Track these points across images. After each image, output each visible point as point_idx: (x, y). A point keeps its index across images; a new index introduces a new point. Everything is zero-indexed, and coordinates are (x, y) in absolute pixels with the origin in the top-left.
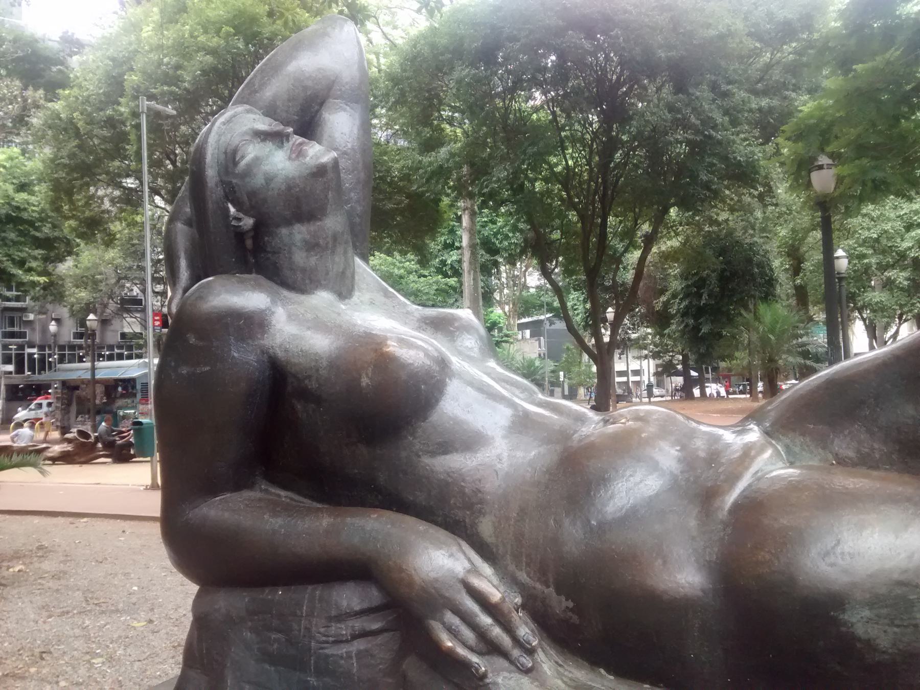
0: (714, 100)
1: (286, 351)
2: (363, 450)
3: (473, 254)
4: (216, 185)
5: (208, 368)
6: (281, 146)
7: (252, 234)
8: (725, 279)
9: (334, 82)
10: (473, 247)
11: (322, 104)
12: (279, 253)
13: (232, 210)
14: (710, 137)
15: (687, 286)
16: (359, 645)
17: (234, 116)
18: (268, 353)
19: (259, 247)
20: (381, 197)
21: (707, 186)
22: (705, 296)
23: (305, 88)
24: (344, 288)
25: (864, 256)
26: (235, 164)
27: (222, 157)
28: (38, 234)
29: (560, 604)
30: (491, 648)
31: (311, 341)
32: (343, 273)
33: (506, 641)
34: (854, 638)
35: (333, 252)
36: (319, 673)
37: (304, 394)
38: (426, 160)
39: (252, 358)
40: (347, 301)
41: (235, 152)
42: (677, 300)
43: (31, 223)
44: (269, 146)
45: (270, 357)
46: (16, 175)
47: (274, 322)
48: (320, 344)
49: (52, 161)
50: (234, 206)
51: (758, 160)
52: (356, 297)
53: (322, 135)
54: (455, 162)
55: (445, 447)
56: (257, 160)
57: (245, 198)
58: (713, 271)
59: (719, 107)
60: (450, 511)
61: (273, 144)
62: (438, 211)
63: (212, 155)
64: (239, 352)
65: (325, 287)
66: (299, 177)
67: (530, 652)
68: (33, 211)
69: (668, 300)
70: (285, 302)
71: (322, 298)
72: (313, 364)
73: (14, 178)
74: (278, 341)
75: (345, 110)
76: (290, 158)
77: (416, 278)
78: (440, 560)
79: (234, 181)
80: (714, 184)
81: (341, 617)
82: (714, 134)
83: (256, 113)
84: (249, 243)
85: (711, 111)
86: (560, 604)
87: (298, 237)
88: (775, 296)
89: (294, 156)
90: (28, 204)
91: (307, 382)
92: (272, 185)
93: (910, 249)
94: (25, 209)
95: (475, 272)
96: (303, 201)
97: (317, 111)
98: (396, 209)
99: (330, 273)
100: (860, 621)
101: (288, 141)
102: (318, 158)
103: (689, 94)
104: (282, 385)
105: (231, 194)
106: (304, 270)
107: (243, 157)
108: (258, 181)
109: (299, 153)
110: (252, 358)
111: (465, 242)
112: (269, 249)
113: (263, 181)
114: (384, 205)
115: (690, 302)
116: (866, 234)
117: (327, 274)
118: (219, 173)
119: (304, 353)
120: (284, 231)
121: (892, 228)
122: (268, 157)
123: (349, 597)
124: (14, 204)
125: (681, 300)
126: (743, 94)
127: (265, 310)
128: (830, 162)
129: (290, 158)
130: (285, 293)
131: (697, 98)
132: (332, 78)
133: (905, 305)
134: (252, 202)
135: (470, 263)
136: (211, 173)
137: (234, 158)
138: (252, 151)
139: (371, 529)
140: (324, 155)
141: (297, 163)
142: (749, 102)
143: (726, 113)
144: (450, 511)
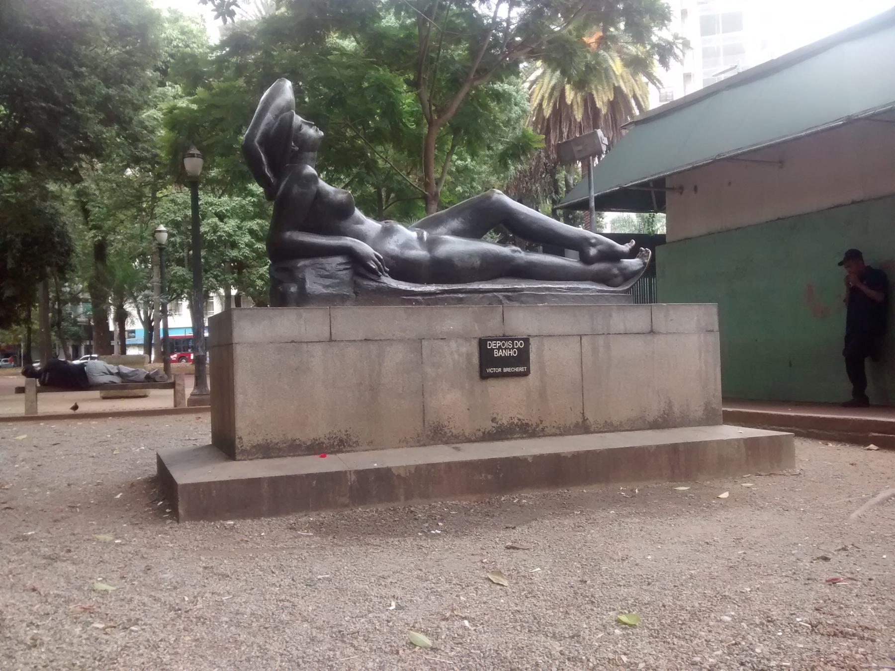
16: (344, 272)
36: (336, 278)
58: (17, 236)
88: (71, 265)
100: (456, 261)
123: (339, 259)
128: (198, 152)
139: (348, 241)
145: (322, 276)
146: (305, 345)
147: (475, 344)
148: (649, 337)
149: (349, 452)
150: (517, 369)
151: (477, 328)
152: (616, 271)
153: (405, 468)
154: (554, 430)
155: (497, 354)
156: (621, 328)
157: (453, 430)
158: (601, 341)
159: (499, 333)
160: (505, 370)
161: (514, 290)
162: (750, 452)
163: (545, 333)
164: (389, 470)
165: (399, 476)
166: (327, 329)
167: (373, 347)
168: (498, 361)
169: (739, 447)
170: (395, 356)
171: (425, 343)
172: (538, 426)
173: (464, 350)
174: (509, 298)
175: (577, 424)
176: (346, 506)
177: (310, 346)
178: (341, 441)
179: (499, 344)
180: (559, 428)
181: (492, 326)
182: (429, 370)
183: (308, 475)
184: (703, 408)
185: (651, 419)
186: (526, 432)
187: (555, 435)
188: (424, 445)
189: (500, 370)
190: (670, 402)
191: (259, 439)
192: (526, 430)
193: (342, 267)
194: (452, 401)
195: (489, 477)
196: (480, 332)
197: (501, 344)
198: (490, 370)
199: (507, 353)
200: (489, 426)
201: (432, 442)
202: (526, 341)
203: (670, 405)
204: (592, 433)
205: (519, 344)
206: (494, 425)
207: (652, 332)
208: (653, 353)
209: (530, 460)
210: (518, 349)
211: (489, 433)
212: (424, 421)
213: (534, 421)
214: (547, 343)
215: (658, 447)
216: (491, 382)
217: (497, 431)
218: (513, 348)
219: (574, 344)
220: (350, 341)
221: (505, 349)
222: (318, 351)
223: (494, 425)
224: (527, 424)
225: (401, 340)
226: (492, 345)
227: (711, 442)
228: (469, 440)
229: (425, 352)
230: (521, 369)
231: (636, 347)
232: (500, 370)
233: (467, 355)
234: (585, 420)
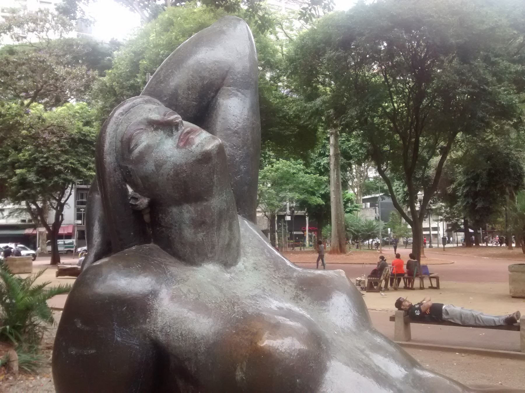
0: (486, 67)
1: (167, 334)
3: (336, 160)
4: (115, 171)
5: (93, 351)
6: (171, 135)
7: (148, 211)
9: (227, 72)
10: (336, 155)
11: (217, 91)
12: (171, 228)
13: (130, 190)
14: (484, 90)
15: (468, 179)
17: (133, 107)
18: (149, 337)
19: (155, 222)
20: (283, 128)
21: (482, 120)
22: (479, 185)
23: (202, 78)
24: (228, 257)
26: (130, 151)
27: (119, 144)
31: (190, 326)
32: (229, 245)
35: (219, 229)
37: (184, 374)
38: (309, 105)
39: (134, 342)
40: (232, 268)
41: (130, 140)
42: (462, 187)
43: (91, 143)
44: (160, 135)
45: (152, 340)
46: (84, 117)
47: (156, 306)
48: (201, 326)
49: (102, 109)
50: (132, 187)
51: (515, 103)
52: (240, 265)
53: (217, 118)
54: (326, 107)
56: (149, 148)
57: (140, 181)
59: (490, 72)
61: (164, 133)
63: (110, 143)
64: (122, 336)
65: (211, 260)
66: (186, 164)
68: (93, 136)
69: (456, 187)
72: (192, 348)
73: (83, 118)
74: (160, 324)
75: (236, 95)
76: (178, 147)
79: (130, 166)
80: (486, 118)
82: (487, 88)
83: (154, 103)
84: (147, 218)
85: (485, 74)
87: (186, 216)
89: (182, 144)
90: (90, 132)
91: (187, 363)
92: (162, 171)
94: (88, 135)
95: (337, 170)
96: (191, 184)
97: (213, 97)
98: (291, 135)
99: (216, 248)
101: (177, 129)
102: (203, 146)
103: (471, 64)
105: (128, 177)
106: (192, 245)
107: (136, 145)
108: (150, 167)
109: (186, 141)
110: (134, 342)
111: (332, 152)
112: (163, 224)
113: (153, 168)
114: (285, 133)
115: (470, 189)
117: (213, 247)
118: (116, 159)
120: (175, 210)
122: (158, 144)
124: (82, 132)
125: (464, 187)
126: (506, 63)
127: (148, 295)
129: (178, 147)
131: (476, 66)
132: (226, 69)
134: (146, 185)
135: (334, 165)
136: (109, 159)
137: (129, 147)
138: (145, 140)
140: (209, 143)
141: (184, 150)
142: (509, 67)
143: (494, 74)
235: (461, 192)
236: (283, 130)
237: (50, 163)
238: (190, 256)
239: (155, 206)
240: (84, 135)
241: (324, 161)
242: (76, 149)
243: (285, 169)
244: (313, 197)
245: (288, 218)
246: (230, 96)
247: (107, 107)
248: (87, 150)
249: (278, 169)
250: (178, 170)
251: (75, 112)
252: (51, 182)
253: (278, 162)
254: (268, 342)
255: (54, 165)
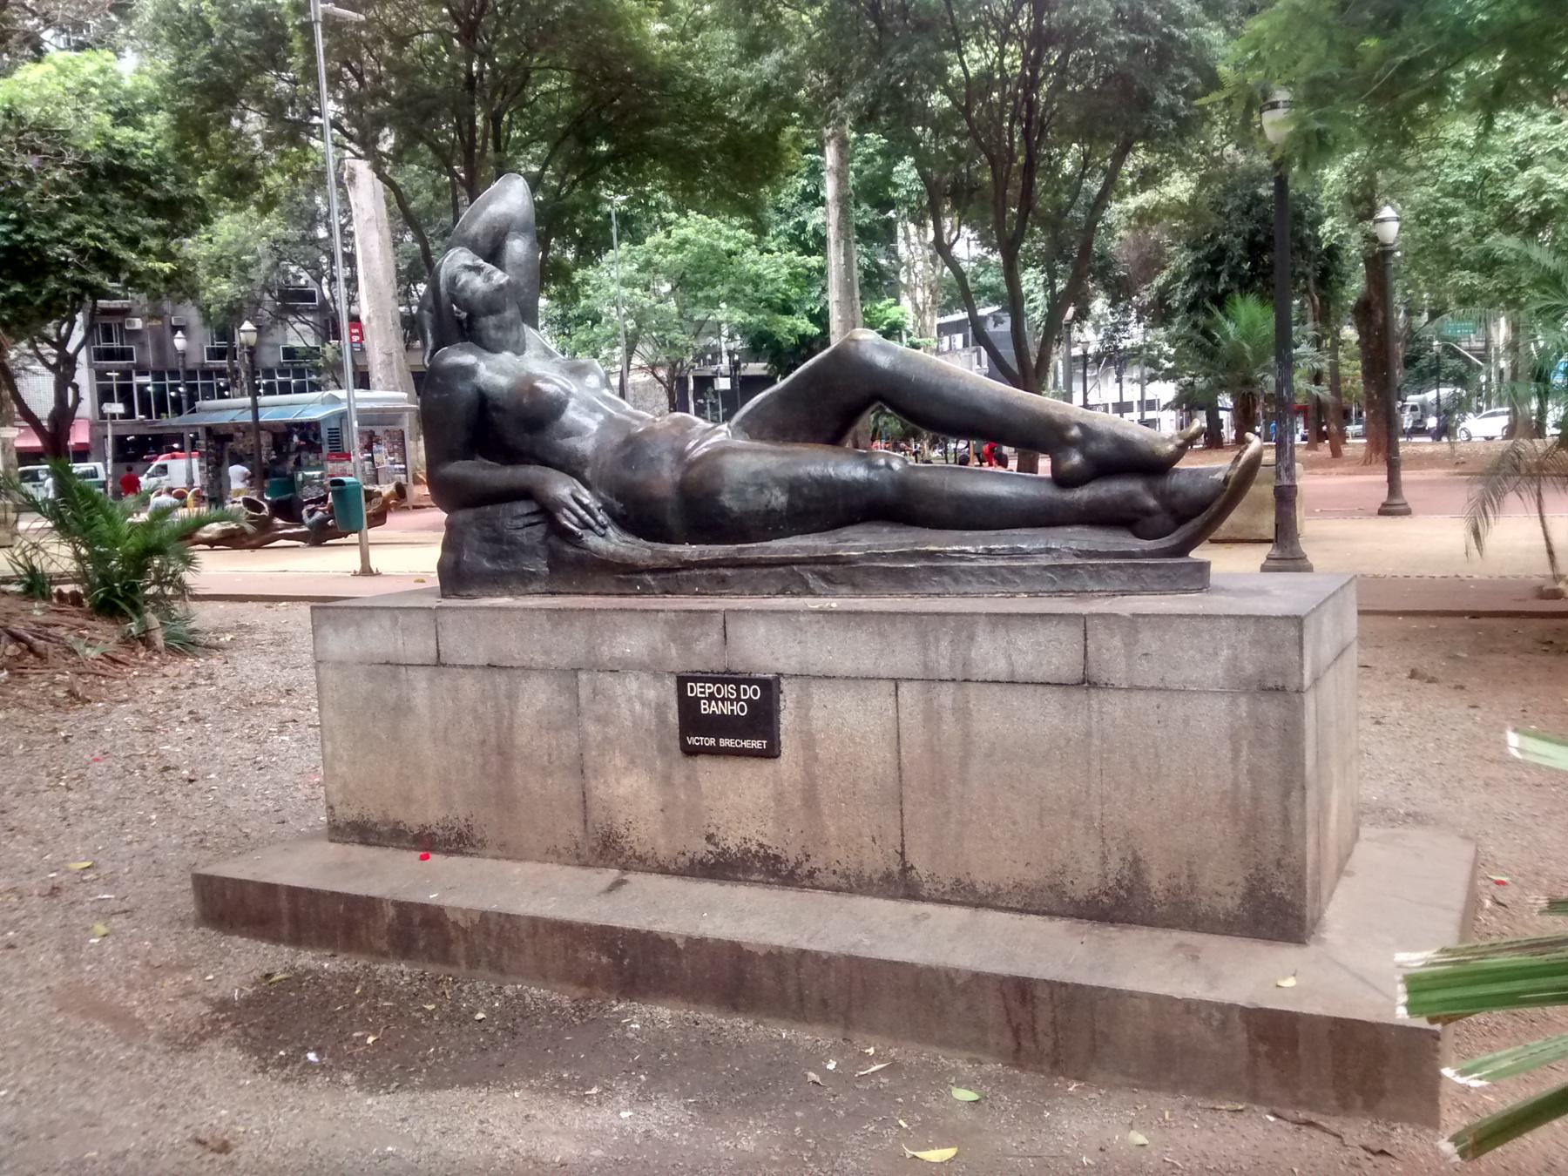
2: (527, 437)
3: (844, 212)
8: (1255, 248)
10: (843, 200)
14: (1171, 37)
15: (1197, 261)
16: (528, 530)
19: (471, 328)
20: (684, 128)
22: (1224, 277)
24: (519, 349)
25: (1454, 212)
28: (155, 194)
29: (618, 506)
30: (586, 526)
33: (592, 522)
34: (723, 507)
37: (497, 408)
38: (745, 75)
42: (1180, 285)
43: (143, 177)
46: (113, 97)
48: (503, 381)
49: (173, 78)
52: (526, 354)
54: (789, 80)
55: (569, 434)
58: (1237, 235)
60: (571, 466)
62: (776, 149)
67: (604, 527)
68: (146, 156)
69: (1167, 283)
70: (484, 359)
71: (506, 357)
73: (110, 102)
77: (756, 256)
78: (563, 488)
81: (518, 517)
82: (1177, 32)
86: (618, 506)
88: (1338, 274)
90: (136, 144)
93: (1519, 199)
94: (132, 154)
95: (848, 243)
96: (493, 304)
104: (484, 403)
105: (454, 300)
108: (468, 294)
109: (488, 278)
111: (830, 190)
115: (1202, 287)
116: (1456, 176)
119: (495, 386)
121: (1498, 166)
123: (522, 508)
125: (1186, 283)
130: (486, 354)
133: (1509, 290)
134: (466, 305)
135: (839, 228)
136: (443, 289)
138: (464, 277)
139: (530, 473)
144: (571, 466)
145: (485, 540)
146: (403, 669)
147: (671, 684)
148: (1078, 696)
149: (471, 855)
150: (746, 744)
151: (674, 652)
152: (1152, 502)
153: (466, 912)
154: (834, 879)
155: (707, 708)
156: (999, 667)
157: (635, 845)
158: (946, 696)
159: (717, 665)
160: (724, 742)
161: (834, 560)
162: (1263, 1048)
163: (814, 670)
164: (440, 910)
165: (455, 923)
166: (433, 643)
167: (501, 679)
168: (730, 721)
169: (1224, 1023)
170: (537, 697)
171: (583, 677)
172: (799, 864)
173: (651, 694)
174: (824, 577)
175: (887, 877)
176: (383, 955)
177: (412, 673)
178: (460, 835)
179: (710, 688)
180: (847, 877)
181: (705, 652)
182: (592, 728)
183: (333, 893)
184: (1240, 890)
185: (1079, 892)
186: (775, 873)
187: (837, 890)
188: (586, 865)
189: (712, 741)
190: (1137, 860)
191: (352, 813)
192: (772, 869)
193: (520, 523)
194: (633, 791)
195: (604, 960)
196: (677, 660)
197: (714, 689)
198: (692, 740)
199: (726, 709)
200: (701, 848)
201: (601, 862)
202: (770, 687)
203: (1136, 864)
204: (924, 900)
205: (751, 692)
206: (711, 848)
207: (1086, 683)
208: (1089, 734)
209: (680, 944)
210: (749, 701)
211: (701, 862)
212: (585, 822)
213: (792, 854)
214: (820, 694)
215: (978, 979)
216: (703, 763)
217: (717, 862)
218: (738, 699)
219: (881, 699)
220: (465, 667)
221: (723, 700)
222: (420, 679)
223: (711, 848)
224: (776, 857)
225: (544, 670)
226: (696, 690)
227: (1132, 995)
228: (663, 870)
229: (584, 693)
230: (756, 744)
231: (1041, 716)
232: (712, 741)
233: (658, 705)
234: (906, 869)
235: (1178, 296)
236: (687, 133)
237: (30, 238)
238: (493, 348)
239: (472, 316)
240: (121, 154)
241: (815, 218)
242: (101, 196)
243: (704, 239)
244: (785, 318)
245: (723, 384)
246: (515, 238)
247: (187, 74)
248: (135, 197)
249: (684, 242)
250: (485, 295)
251: (83, 84)
252: (39, 293)
253: (683, 221)
254: (539, 384)
255: (44, 242)
